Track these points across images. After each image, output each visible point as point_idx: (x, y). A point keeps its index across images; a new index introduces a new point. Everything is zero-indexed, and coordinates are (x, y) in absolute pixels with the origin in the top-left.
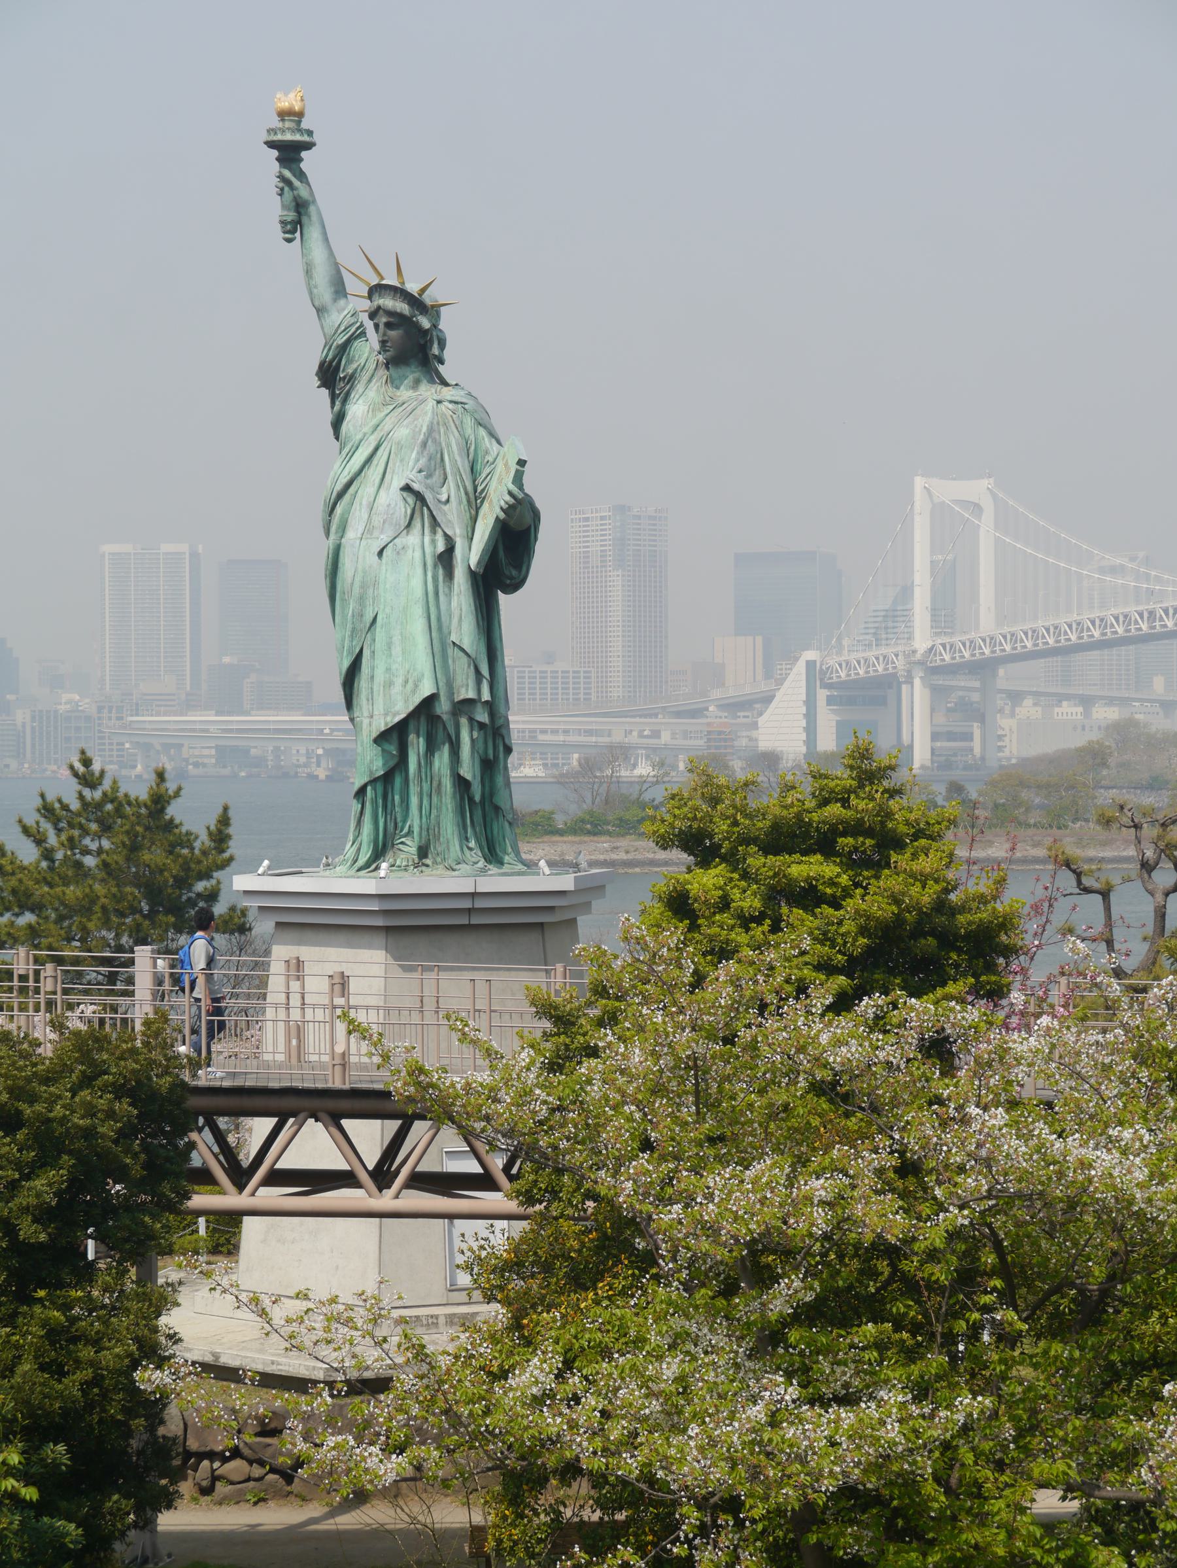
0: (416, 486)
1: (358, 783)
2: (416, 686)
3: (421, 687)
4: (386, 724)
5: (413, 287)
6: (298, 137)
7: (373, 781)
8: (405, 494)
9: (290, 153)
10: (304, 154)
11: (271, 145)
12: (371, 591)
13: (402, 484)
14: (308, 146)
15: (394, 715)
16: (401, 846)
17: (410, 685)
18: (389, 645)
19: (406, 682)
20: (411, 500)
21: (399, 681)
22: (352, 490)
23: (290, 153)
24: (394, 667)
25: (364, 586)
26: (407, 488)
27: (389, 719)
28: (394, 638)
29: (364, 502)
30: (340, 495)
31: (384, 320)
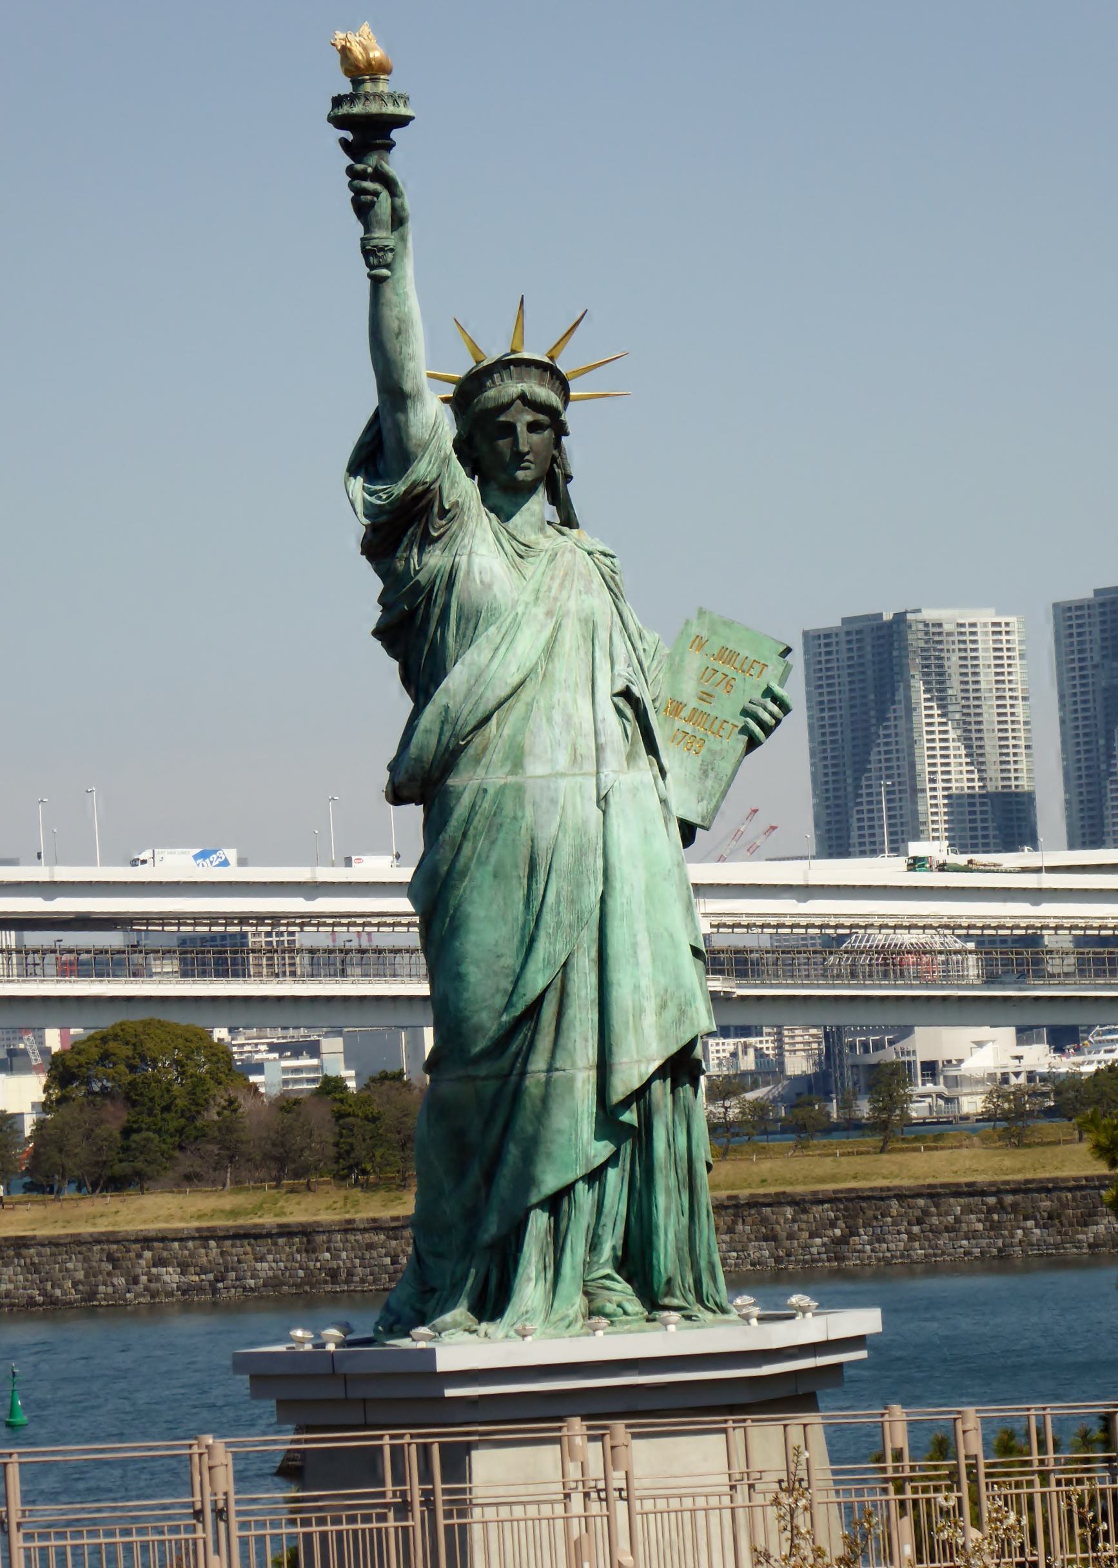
0: (636, 690)
1: (550, 1181)
2: (682, 1012)
3: (691, 1012)
4: (641, 1077)
5: (563, 366)
6: (390, 109)
7: (582, 1178)
8: (621, 702)
9: (367, 135)
10: (395, 134)
11: (339, 122)
12: (591, 860)
13: (620, 686)
14: (402, 121)
15: (649, 1061)
16: (608, 1283)
17: (672, 1011)
18: (635, 945)
19: (663, 1006)
20: (629, 712)
21: (651, 1006)
22: (525, 695)
23: (367, 135)
24: (644, 982)
25: (580, 853)
26: (626, 694)
27: (643, 1068)
28: (639, 938)
29: (557, 717)
30: (500, 705)
31: (529, 417)
